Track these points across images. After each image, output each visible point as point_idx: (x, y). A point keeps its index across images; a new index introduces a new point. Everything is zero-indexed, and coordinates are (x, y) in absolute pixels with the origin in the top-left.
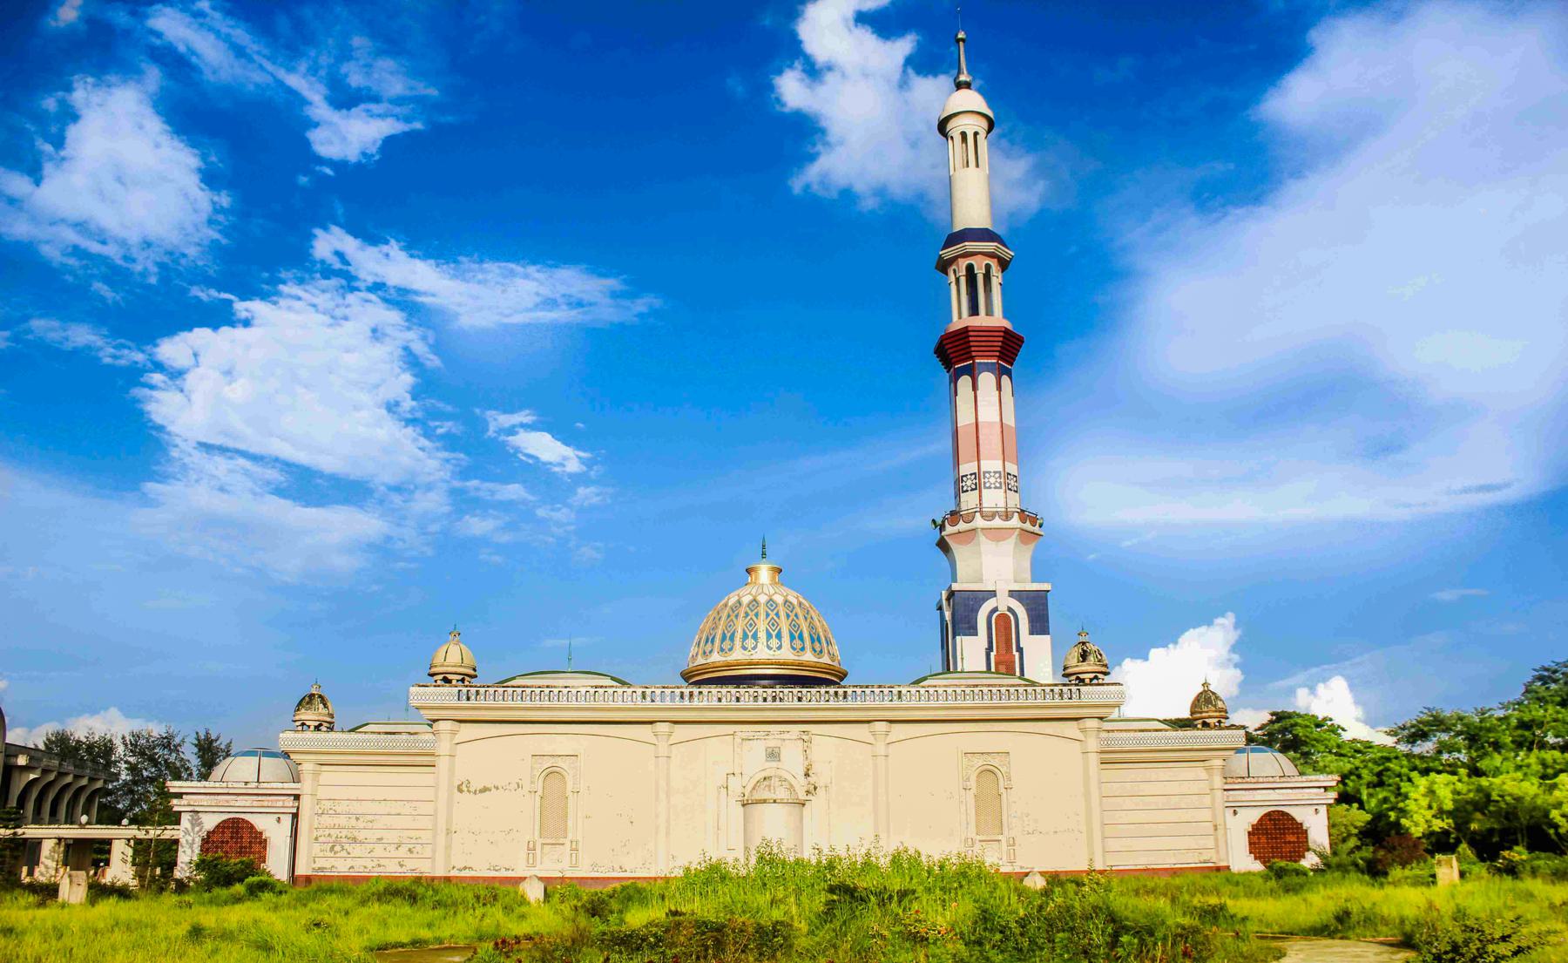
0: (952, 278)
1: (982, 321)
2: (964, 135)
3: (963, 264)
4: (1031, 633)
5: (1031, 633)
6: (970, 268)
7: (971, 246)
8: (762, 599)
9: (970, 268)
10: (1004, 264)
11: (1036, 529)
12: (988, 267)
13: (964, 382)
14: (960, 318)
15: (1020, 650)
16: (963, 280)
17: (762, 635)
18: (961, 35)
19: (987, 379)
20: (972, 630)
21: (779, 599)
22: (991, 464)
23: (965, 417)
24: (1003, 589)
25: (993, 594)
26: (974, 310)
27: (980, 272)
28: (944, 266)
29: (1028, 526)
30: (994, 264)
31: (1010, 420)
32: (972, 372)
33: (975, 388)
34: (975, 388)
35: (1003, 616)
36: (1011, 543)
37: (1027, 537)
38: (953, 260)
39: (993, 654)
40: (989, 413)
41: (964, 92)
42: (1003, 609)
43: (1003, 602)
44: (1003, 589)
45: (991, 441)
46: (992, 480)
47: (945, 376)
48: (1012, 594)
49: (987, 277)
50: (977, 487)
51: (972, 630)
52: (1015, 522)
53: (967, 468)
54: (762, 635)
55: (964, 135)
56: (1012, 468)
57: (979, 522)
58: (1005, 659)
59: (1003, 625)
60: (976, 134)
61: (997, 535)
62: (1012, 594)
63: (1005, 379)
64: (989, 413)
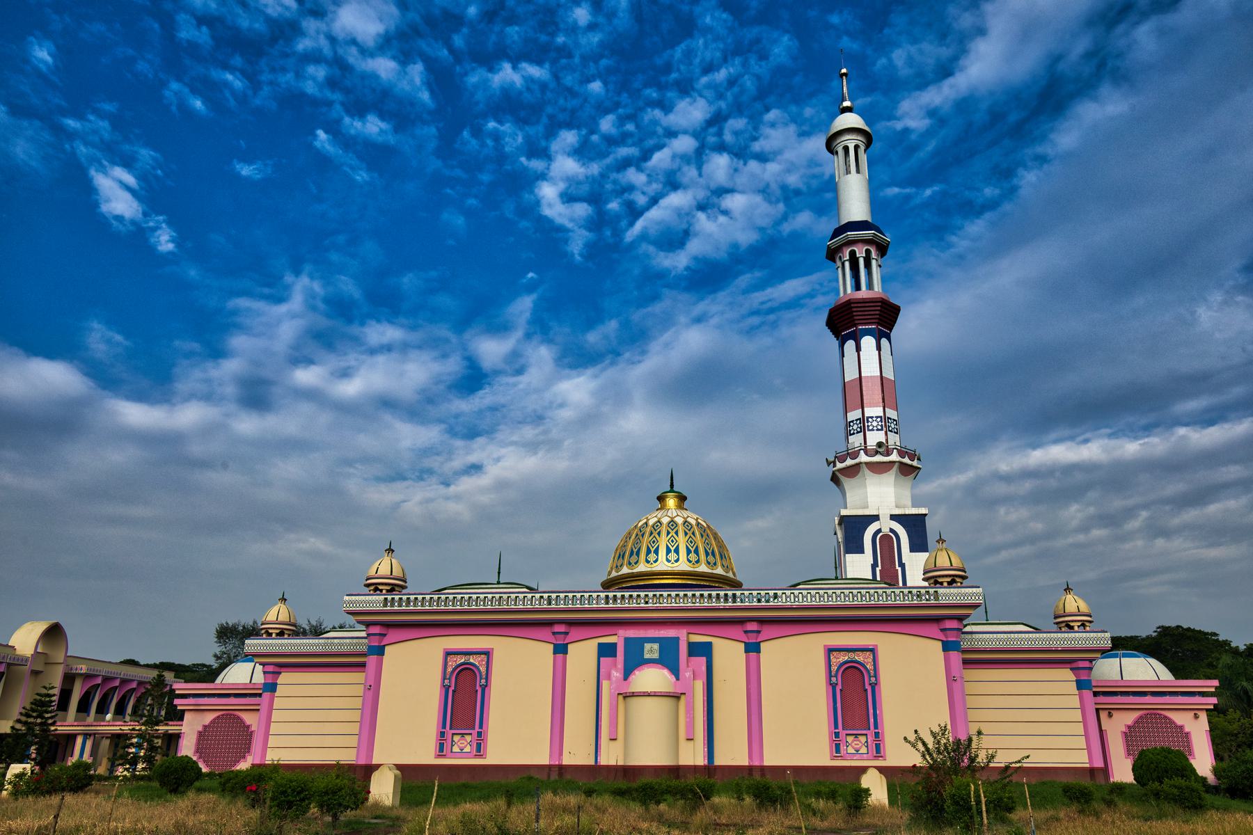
0: (839, 264)
1: (864, 293)
6: (853, 254)
7: (851, 234)
8: (665, 520)
9: (853, 254)
10: (883, 249)
11: (915, 463)
12: (868, 252)
13: (850, 345)
14: (846, 290)
15: (902, 565)
16: (847, 264)
17: (662, 552)
18: (844, 71)
19: (868, 342)
20: (860, 550)
21: (679, 520)
23: (851, 375)
24: (885, 514)
25: (876, 518)
26: (857, 287)
27: (860, 252)
28: (832, 254)
29: (906, 460)
34: (858, 349)
35: (886, 538)
37: (906, 470)
38: (839, 249)
39: (878, 569)
40: (870, 368)
41: (848, 115)
42: (886, 530)
43: (886, 525)
44: (885, 514)
46: (875, 424)
47: (833, 342)
48: (893, 517)
50: (863, 430)
51: (860, 550)
54: (662, 552)
55: (846, 149)
57: (863, 458)
58: (889, 571)
60: (856, 147)
62: (893, 517)
63: (884, 341)
64: (870, 368)
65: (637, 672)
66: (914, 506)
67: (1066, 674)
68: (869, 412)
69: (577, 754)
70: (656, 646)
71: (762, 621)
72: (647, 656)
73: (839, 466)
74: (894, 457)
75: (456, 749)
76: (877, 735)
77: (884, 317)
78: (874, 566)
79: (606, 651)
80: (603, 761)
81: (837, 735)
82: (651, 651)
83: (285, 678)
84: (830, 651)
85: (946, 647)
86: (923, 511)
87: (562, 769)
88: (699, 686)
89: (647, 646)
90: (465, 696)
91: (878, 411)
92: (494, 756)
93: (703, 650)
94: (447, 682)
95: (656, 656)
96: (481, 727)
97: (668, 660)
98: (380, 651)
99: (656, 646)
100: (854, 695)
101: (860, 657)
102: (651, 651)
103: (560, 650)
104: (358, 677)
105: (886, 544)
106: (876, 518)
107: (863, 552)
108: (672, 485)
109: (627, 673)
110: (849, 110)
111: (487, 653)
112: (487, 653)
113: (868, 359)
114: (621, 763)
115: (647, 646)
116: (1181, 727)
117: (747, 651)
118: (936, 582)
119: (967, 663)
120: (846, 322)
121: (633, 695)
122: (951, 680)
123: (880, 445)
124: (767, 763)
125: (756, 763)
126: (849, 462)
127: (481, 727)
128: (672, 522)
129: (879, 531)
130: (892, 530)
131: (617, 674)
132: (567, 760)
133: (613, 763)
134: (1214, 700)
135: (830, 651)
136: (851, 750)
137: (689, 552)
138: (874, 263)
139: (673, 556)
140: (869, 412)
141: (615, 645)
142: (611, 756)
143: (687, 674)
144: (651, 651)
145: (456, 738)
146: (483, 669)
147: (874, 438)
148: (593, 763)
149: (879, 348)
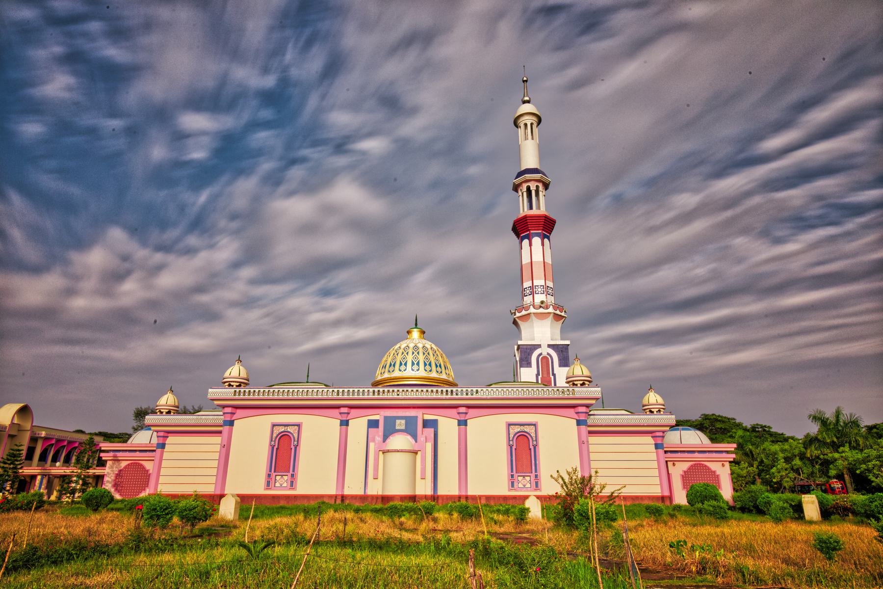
0: (520, 193)
1: (535, 212)
2: (526, 125)
3: (525, 186)
4: (560, 366)
5: (560, 366)
8: (412, 345)
9: (528, 189)
10: (546, 186)
11: (563, 314)
12: (537, 187)
13: (526, 242)
14: (524, 210)
15: (554, 375)
16: (525, 194)
17: (409, 364)
19: (536, 241)
20: (529, 365)
21: (420, 346)
23: (526, 260)
27: (533, 188)
28: (516, 188)
29: (558, 312)
30: (540, 185)
31: (549, 260)
32: (529, 238)
33: (530, 245)
34: (530, 245)
35: (545, 359)
36: (549, 321)
37: (557, 317)
38: (520, 185)
40: (538, 257)
43: (545, 351)
45: (538, 271)
47: (517, 241)
48: (549, 346)
51: (529, 365)
52: (551, 310)
53: (527, 284)
54: (409, 364)
55: (526, 125)
56: (550, 284)
57: (532, 310)
58: (546, 378)
59: (545, 361)
60: (532, 124)
62: (549, 346)
63: (546, 240)
64: (538, 257)
65: (391, 438)
66: (562, 339)
67: (649, 439)
68: (536, 283)
69: (353, 488)
70: (403, 422)
71: (469, 407)
72: (397, 428)
73: (518, 315)
74: (551, 310)
75: (277, 485)
76: (536, 476)
77: (547, 225)
78: (538, 375)
79: (373, 424)
80: (370, 492)
81: (512, 476)
82: (400, 424)
83: (171, 439)
84: (509, 425)
85: (579, 423)
86: (567, 342)
87: (343, 498)
88: (429, 447)
89: (398, 422)
90: (284, 452)
91: (542, 282)
92: (302, 489)
94: (273, 443)
95: (403, 427)
96: (294, 471)
97: (411, 430)
98: (231, 423)
99: (403, 422)
100: (523, 451)
101: (527, 429)
102: (400, 424)
103: (345, 423)
104: (217, 439)
105: (545, 361)
106: (539, 346)
107: (531, 366)
108: (416, 324)
109: (385, 438)
110: (528, 102)
111: (299, 426)
112: (299, 426)
113: (536, 251)
114: (380, 493)
115: (398, 422)
116: (714, 472)
117: (459, 425)
118: (574, 384)
119: (590, 433)
120: (522, 228)
121: (388, 451)
122: (582, 443)
123: (542, 302)
124: (470, 493)
125: (464, 493)
126: (524, 313)
127: (294, 471)
128: (416, 347)
129: (541, 354)
130: (548, 354)
131: (379, 439)
132: (347, 492)
133: (375, 493)
134: (734, 456)
136: (520, 485)
137: (425, 365)
138: (541, 193)
139: (415, 367)
140: (536, 283)
141: (377, 421)
142: (375, 489)
143: (421, 438)
144: (400, 424)
145: (278, 478)
146: (296, 435)
147: (539, 298)
148: (362, 493)
149: (543, 244)
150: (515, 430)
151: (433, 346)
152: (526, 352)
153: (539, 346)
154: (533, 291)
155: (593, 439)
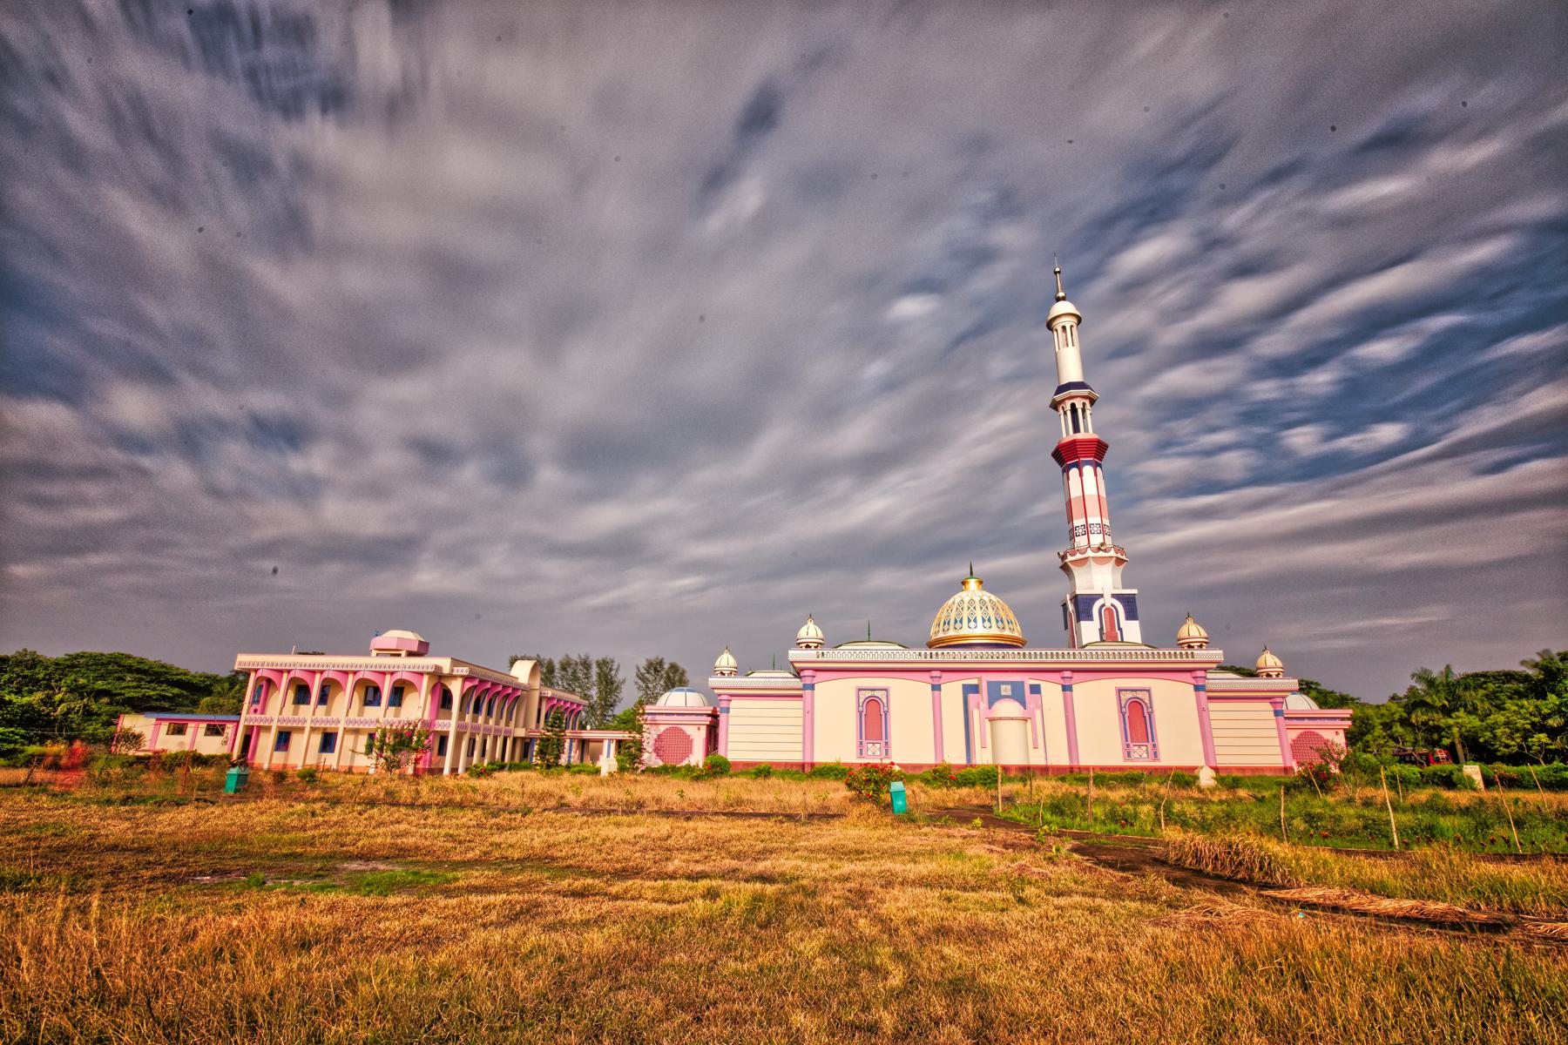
1: (1081, 436)
7: (1073, 392)
9: (1073, 405)
10: (1092, 402)
13: (1074, 472)
14: (1068, 435)
19: (1088, 470)
20: (1089, 617)
22: (1094, 519)
23: (1075, 492)
26: (1076, 429)
27: (1079, 406)
31: (1103, 494)
32: (1079, 466)
33: (1081, 475)
34: (1081, 475)
36: (1111, 565)
37: (1119, 561)
38: (1063, 401)
42: (1108, 605)
45: (1092, 507)
48: (1114, 596)
49: (1084, 411)
50: (1087, 533)
52: (1112, 553)
55: (1064, 328)
58: (1110, 634)
59: (1111, 612)
61: (1101, 561)
62: (1114, 596)
66: (1124, 587)
68: (1090, 521)
74: (1112, 553)
77: (1098, 450)
84: (1120, 691)
85: (1197, 688)
86: (1134, 591)
93: (1036, 689)
97: (1018, 695)
106: (1101, 596)
110: (1064, 299)
113: (1087, 482)
119: (1210, 698)
122: (1202, 711)
126: (1078, 556)
135: (1120, 691)
140: (1090, 521)
143: (1030, 705)
147: (1096, 539)
150: (1126, 696)
151: (993, 598)
152: (1083, 605)
153: (1101, 596)
154: (1087, 529)
155: (1213, 706)
